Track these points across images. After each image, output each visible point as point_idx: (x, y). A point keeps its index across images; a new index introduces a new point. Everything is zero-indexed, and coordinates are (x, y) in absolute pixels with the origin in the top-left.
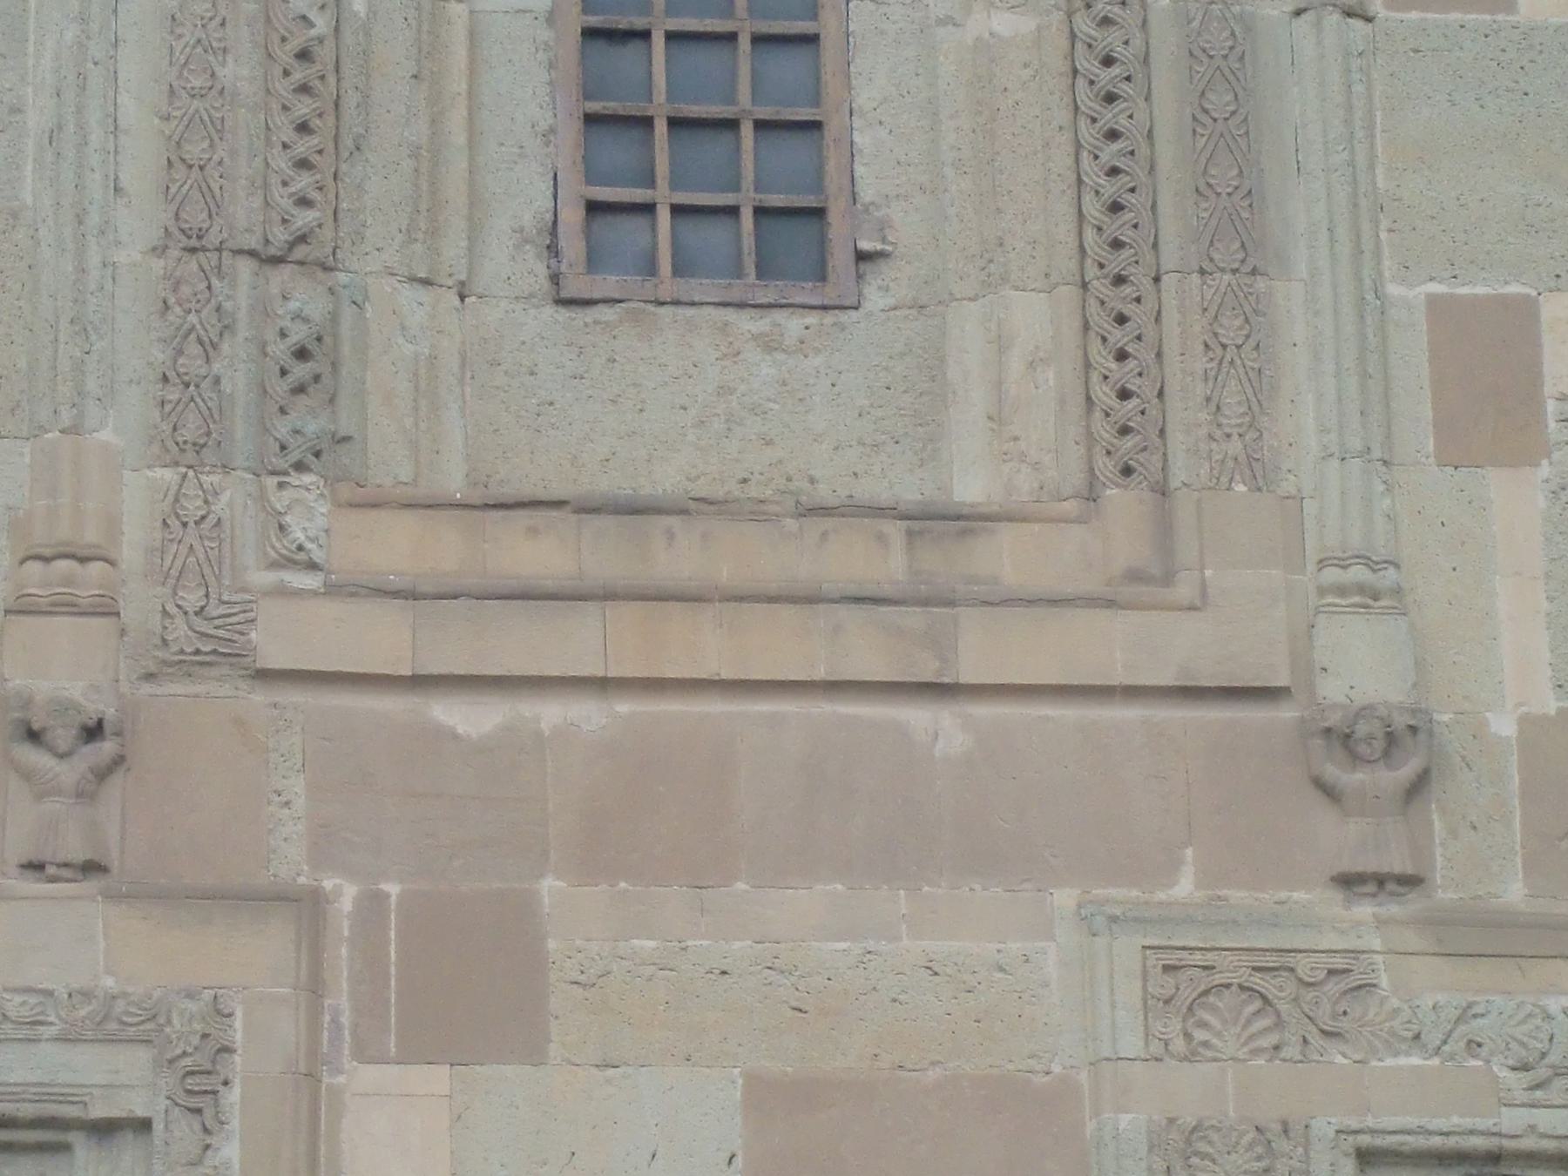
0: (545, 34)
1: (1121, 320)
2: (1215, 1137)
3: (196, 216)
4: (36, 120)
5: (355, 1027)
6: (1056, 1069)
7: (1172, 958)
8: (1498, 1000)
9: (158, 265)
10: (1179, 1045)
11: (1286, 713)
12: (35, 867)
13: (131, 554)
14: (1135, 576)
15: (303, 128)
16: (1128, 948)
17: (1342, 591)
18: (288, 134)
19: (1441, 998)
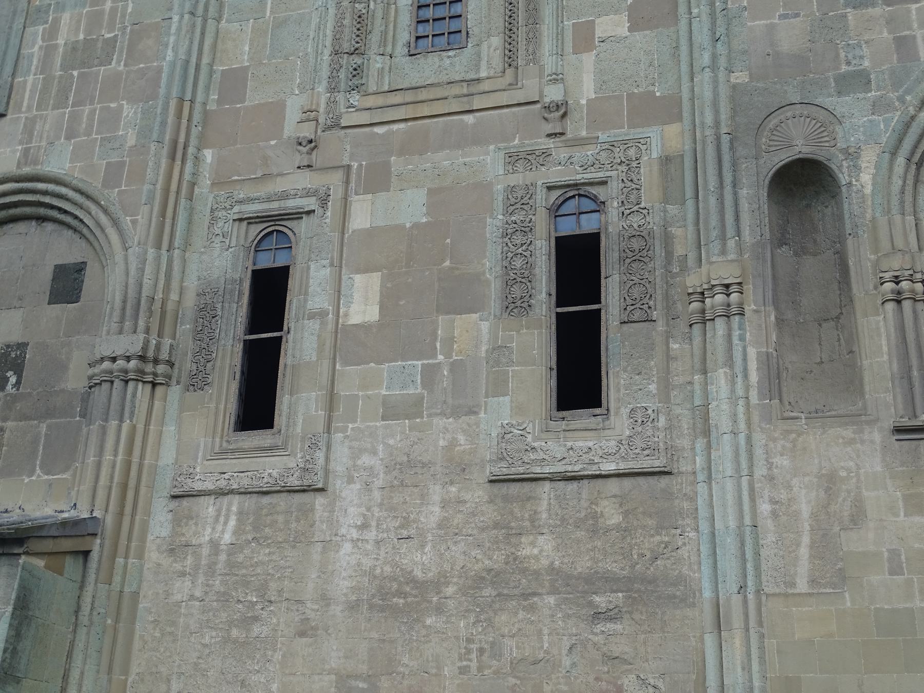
0: (411, 8)
1: (510, 37)
2: (517, 188)
3: (337, 48)
4: (311, 37)
5: (355, 189)
6: (488, 179)
7: (510, 155)
8: (577, 154)
9: (330, 58)
10: (511, 171)
11: (538, 106)
12: (299, 167)
13: (322, 110)
14: (510, 85)
15: (358, 29)
16: (502, 154)
17: (551, 81)
18: (356, 31)
19: (565, 155)
